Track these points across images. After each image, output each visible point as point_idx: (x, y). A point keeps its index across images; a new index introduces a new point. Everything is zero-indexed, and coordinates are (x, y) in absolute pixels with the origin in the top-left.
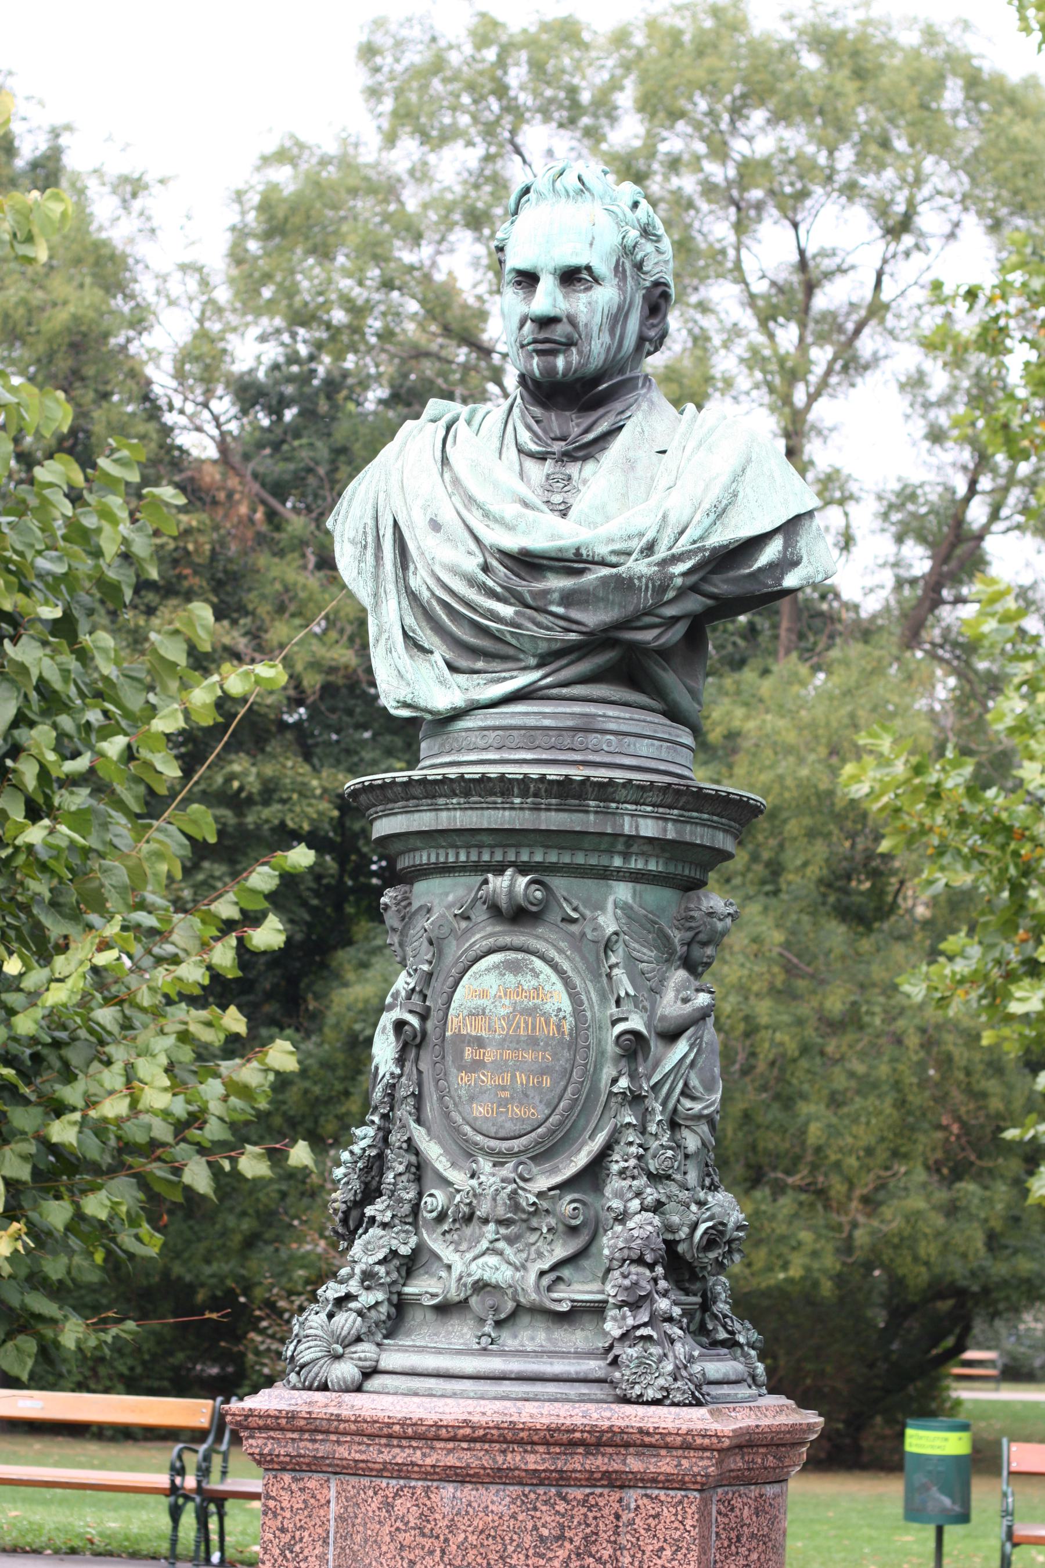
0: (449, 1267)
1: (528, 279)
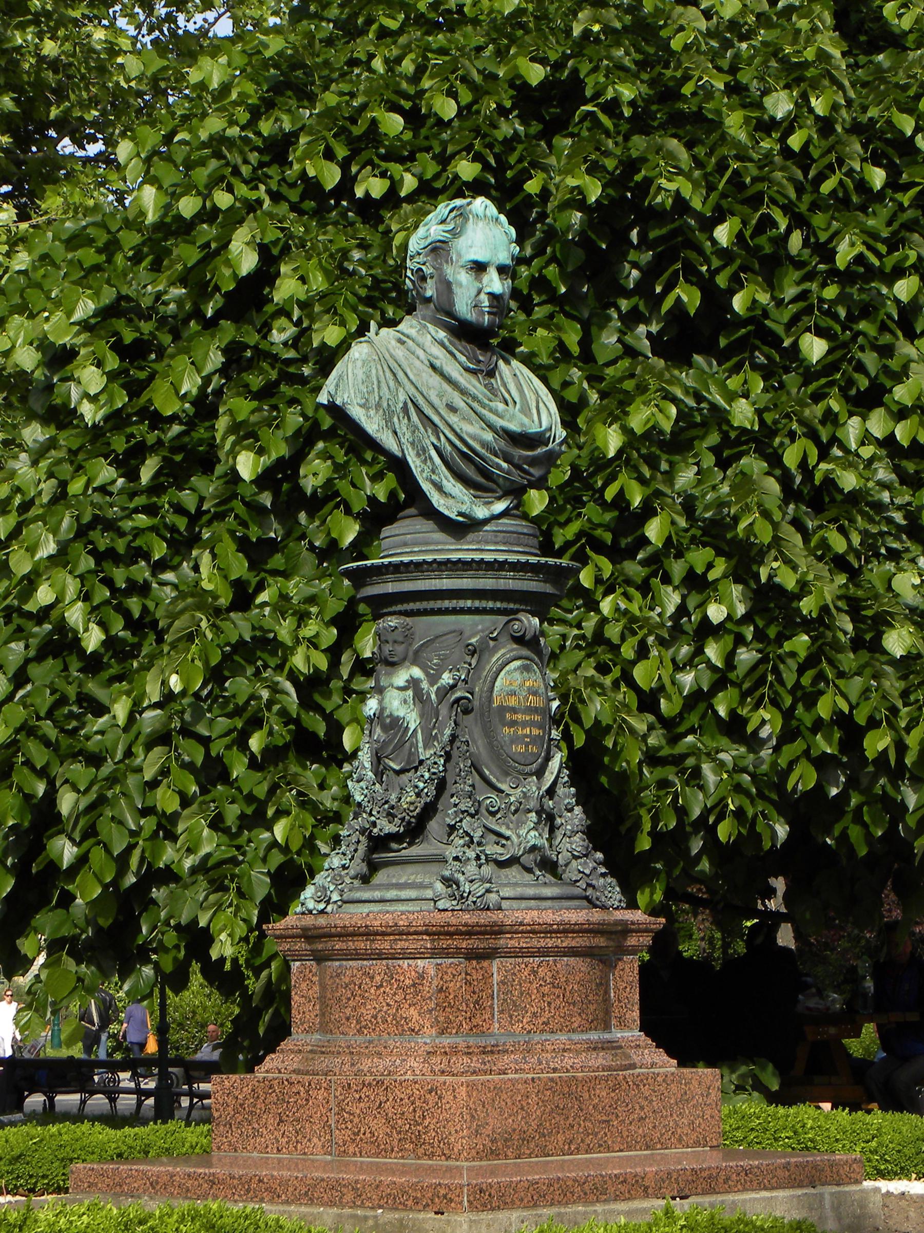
0: (508, 838)
1: (479, 268)
